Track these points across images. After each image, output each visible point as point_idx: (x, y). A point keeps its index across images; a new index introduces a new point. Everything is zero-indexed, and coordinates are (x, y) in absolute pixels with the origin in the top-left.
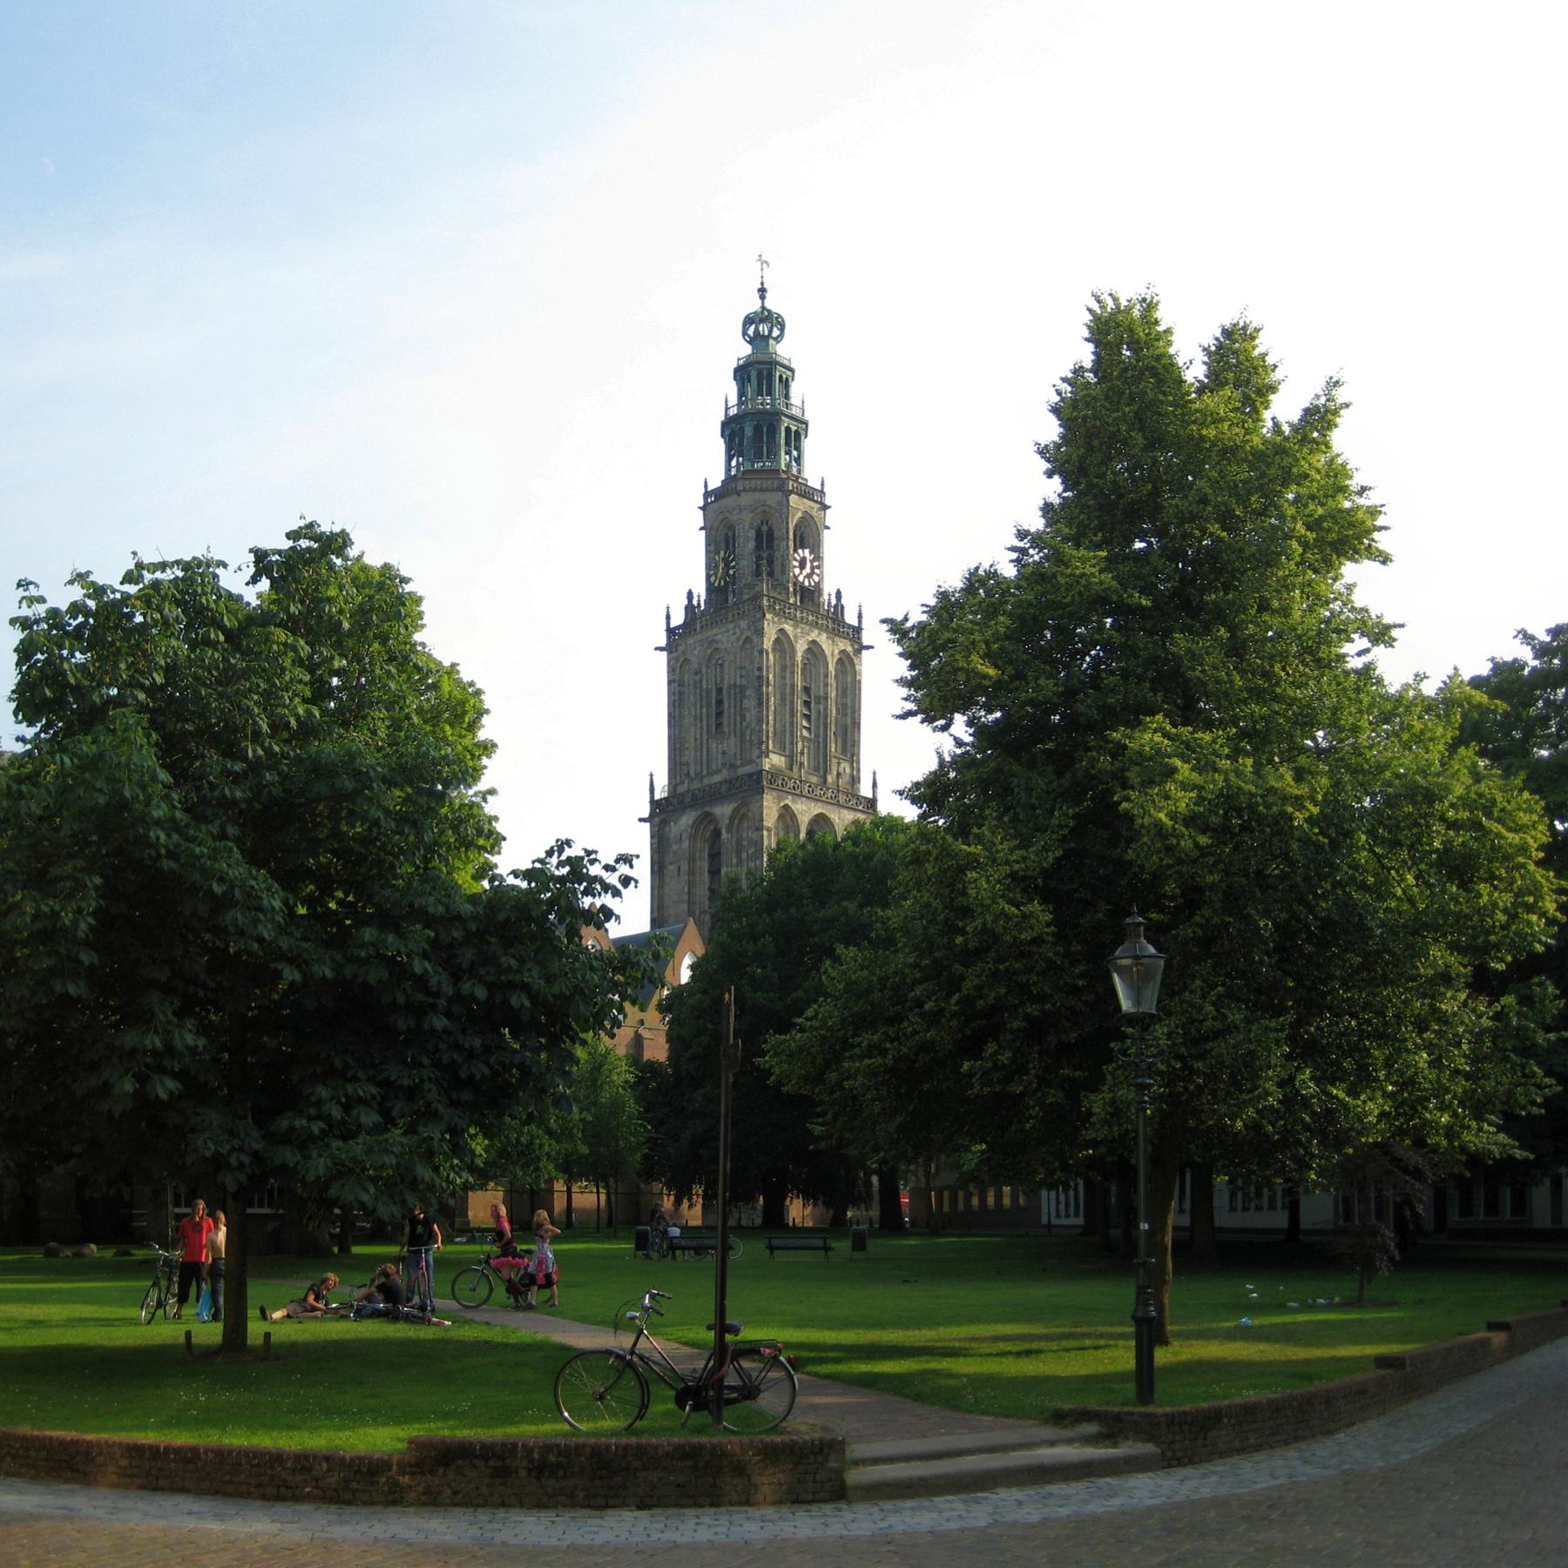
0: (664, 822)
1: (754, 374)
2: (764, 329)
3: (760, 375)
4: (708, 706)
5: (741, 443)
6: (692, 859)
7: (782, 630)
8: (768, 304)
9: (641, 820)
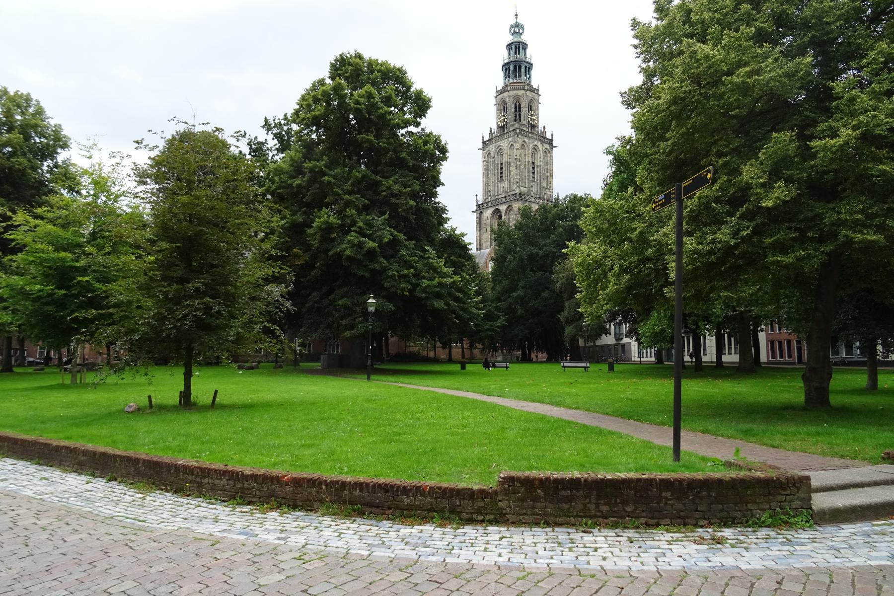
0: (481, 213)
2: (517, 30)
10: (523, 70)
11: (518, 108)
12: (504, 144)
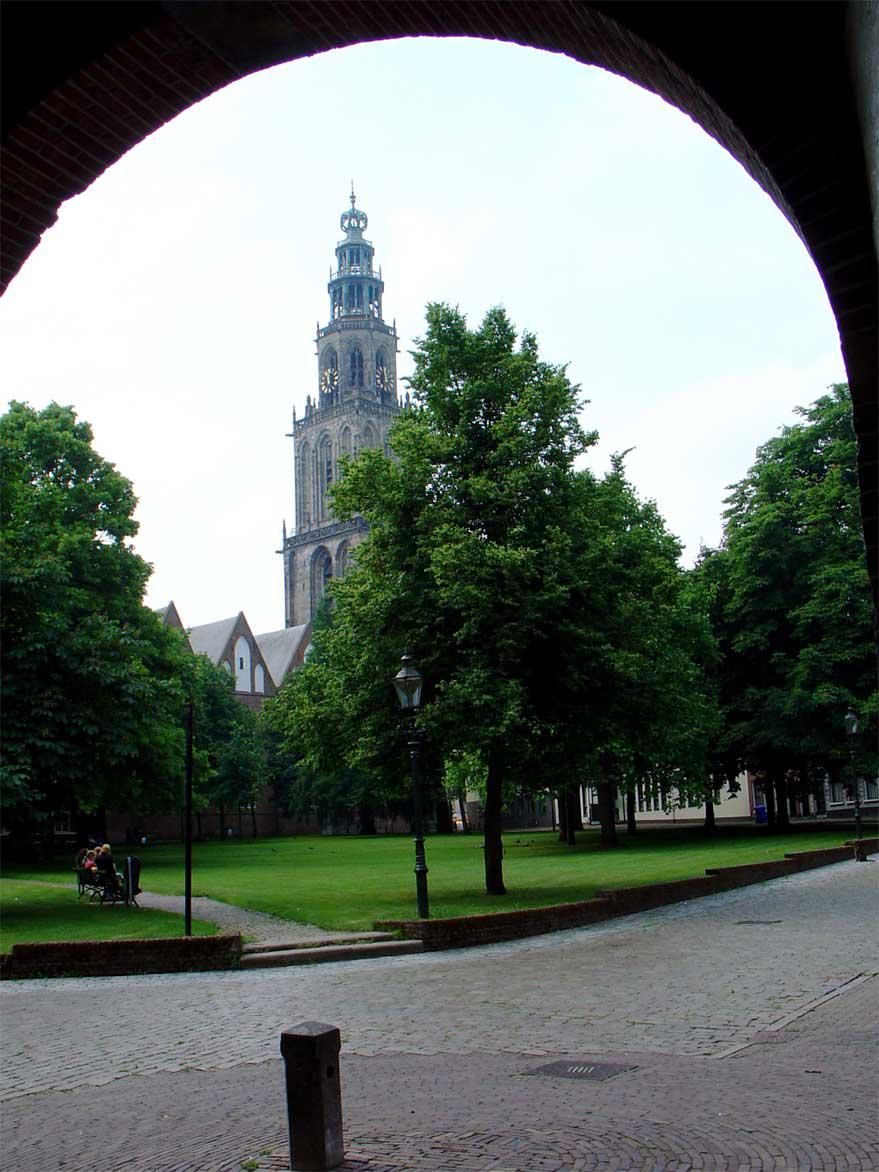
0: (293, 554)
1: (347, 252)
2: (354, 222)
3: (352, 253)
4: (322, 473)
5: (340, 298)
6: (312, 579)
7: (369, 422)
8: (357, 207)
9: (277, 552)
10: (366, 293)
11: (357, 361)
12: (333, 427)
